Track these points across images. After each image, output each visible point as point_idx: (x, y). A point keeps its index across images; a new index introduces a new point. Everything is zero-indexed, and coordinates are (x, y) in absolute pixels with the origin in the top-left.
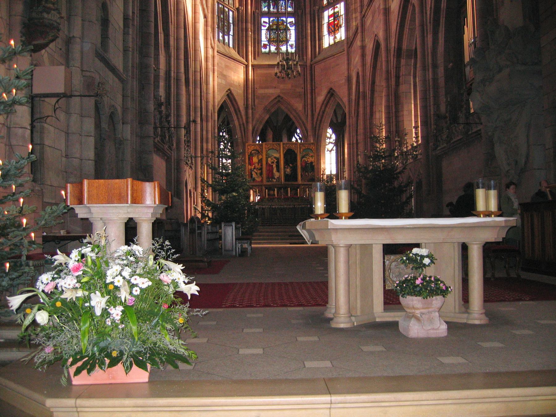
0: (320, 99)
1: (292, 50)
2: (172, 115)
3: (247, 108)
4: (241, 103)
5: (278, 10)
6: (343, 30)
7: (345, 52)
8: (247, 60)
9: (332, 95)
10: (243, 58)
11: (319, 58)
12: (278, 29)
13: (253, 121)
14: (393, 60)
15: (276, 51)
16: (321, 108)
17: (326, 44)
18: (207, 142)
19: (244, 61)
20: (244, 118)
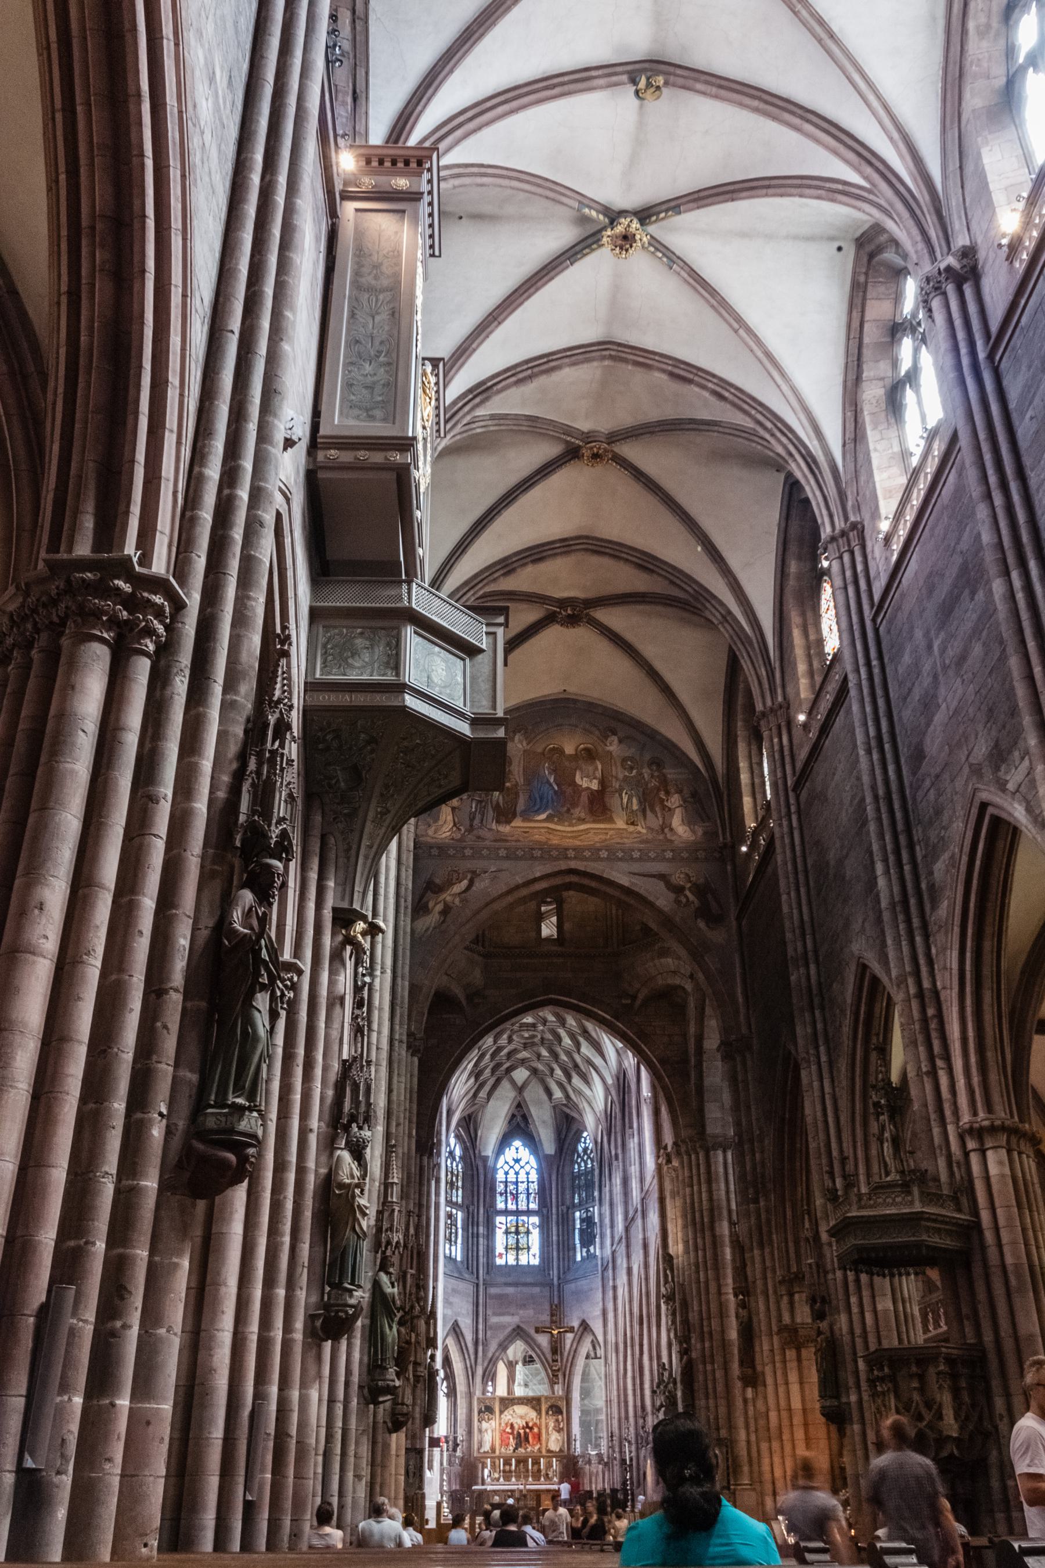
1: (535, 1261)
3: (476, 1343)
4: (469, 1337)
7: (600, 1275)
11: (569, 1277)
12: (517, 1233)
17: (579, 1258)
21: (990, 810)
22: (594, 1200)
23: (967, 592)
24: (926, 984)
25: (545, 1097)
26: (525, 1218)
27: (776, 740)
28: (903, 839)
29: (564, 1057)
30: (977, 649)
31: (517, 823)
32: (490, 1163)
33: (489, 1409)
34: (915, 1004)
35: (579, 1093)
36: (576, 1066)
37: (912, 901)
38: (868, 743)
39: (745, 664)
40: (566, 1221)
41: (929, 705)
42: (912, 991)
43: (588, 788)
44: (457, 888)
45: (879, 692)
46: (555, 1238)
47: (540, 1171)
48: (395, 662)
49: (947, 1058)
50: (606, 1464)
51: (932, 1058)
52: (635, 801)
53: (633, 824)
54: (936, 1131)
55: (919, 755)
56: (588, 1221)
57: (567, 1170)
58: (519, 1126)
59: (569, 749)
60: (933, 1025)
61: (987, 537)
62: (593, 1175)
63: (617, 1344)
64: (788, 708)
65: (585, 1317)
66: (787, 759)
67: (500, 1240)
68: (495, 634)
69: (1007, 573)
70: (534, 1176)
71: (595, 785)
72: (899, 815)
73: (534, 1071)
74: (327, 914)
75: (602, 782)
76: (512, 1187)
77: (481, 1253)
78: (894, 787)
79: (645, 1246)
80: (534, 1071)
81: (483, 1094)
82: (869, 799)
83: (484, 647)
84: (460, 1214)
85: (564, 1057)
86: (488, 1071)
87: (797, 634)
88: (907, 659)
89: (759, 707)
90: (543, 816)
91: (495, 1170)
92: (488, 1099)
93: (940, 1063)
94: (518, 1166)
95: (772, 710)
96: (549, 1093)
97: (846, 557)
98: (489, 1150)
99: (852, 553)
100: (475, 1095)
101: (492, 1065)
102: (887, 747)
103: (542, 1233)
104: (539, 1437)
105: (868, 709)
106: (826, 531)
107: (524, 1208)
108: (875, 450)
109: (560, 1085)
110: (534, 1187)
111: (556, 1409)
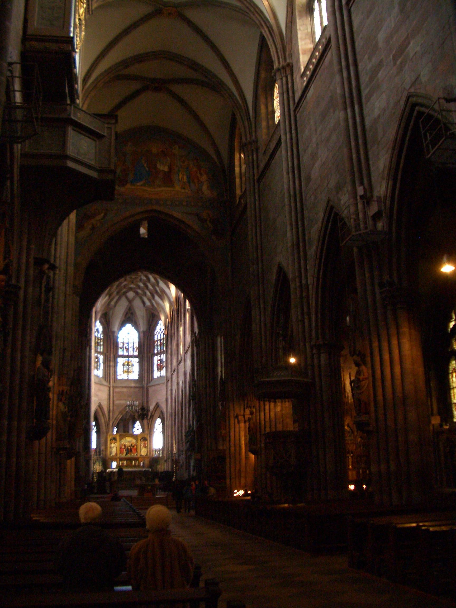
3: (109, 412)
4: (106, 410)
6: (165, 369)
7: (165, 384)
8: (110, 384)
9: (158, 406)
11: (151, 384)
12: (128, 365)
13: (113, 418)
15: (127, 378)
20: (107, 418)
21: (334, 209)
23: (332, 110)
24: (304, 282)
25: (141, 305)
27: (250, 157)
28: (299, 216)
29: (150, 287)
30: (334, 138)
31: (128, 186)
34: (298, 290)
35: (158, 304)
36: (157, 292)
37: (301, 244)
38: (288, 169)
39: (238, 118)
41: (314, 156)
42: (298, 284)
43: (163, 170)
44: (99, 218)
45: (295, 146)
46: (146, 368)
47: (139, 337)
48: (64, 144)
49: (309, 314)
51: (303, 314)
52: (185, 177)
53: (184, 188)
54: (302, 344)
55: (309, 179)
58: (129, 318)
59: (154, 151)
60: (305, 300)
61: (339, 91)
64: (257, 141)
65: (158, 401)
66: (255, 167)
67: (120, 368)
68: (110, 128)
69: (345, 109)
70: (137, 340)
71: (166, 169)
72: (298, 204)
73: (137, 293)
74: (32, 260)
75: (170, 168)
76: (125, 345)
77: (111, 374)
78: (298, 192)
79: (185, 374)
80: (137, 293)
81: (113, 303)
82: (286, 196)
83: (105, 134)
85: (150, 287)
86: (115, 293)
87: (263, 108)
88: (307, 133)
89: (244, 140)
90: (141, 183)
91: (117, 338)
93: (306, 317)
94: (128, 336)
95: (250, 143)
96: (144, 303)
97: (284, 79)
98: (115, 329)
99: (287, 77)
100: (109, 304)
101: (117, 290)
102: (296, 172)
103: (140, 365)
104: (136, 450)
105: (289, 154)
106: (276, 65)
108: (300, 29)
109: (150, 300)
110: (136, 345)
111: (144, 439)
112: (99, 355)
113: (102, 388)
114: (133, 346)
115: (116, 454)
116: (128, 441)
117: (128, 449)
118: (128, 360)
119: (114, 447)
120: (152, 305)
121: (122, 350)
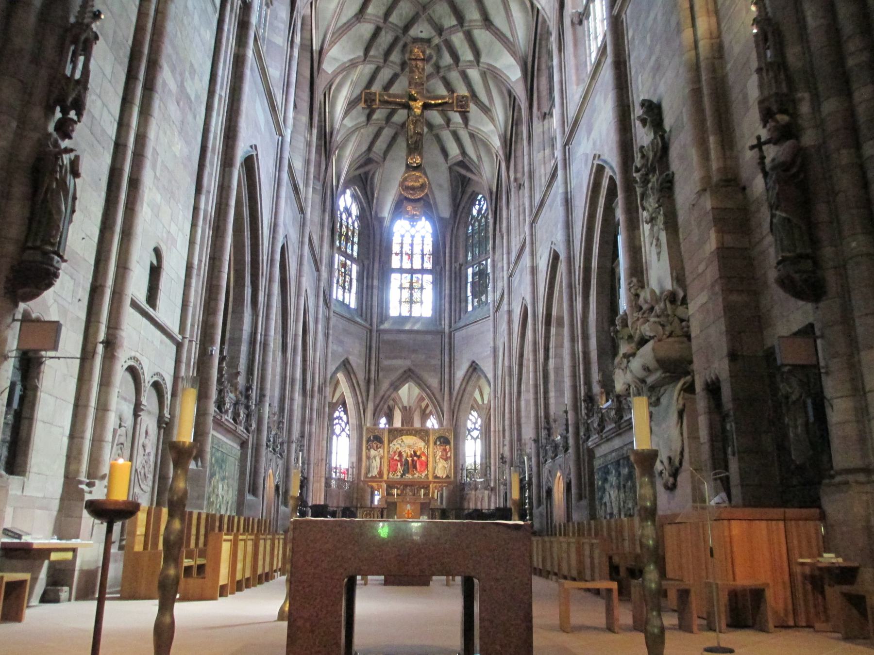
0: (460, 374)
2: (254, 387)
3: (368, 382)
5: (412, 264)
7: (491, 317)
8: (371, 325)
10: (366, 320)
11: (461, 324)
13: (375, 397)
14: (541, 327)
15: (408, 315)
16: (461, 385)
17: (470, 308)
18: (311, 423)
19: (368, 326)
20: (364, 394)
22: (487, 252)
25: (440, 158)
26: (419, 276)
32: (386, 223)
33: (378, 439)
40: (458, 277)
46: (447, 292)
47: (435, 235)
50: (492, 489)
56: (482, 274)
57: (461, 231)
62: (487, 231)
63: (510, 368)
76: (407, 249)
84: (355, 268)
92: (384, 159)
96: (445, 153)
98: (386, 212)
104: (426, 464)
107: (420, 267)
110: (429, 248)
112: (349, 263)
113: (353, 328)
114: (422, 251)
115: (380, 473)
116: (409, 444)
117: (407, 461)
118: (412, 279)
119: (375, 457)
120: (464, 153)
121: (399, 257)
